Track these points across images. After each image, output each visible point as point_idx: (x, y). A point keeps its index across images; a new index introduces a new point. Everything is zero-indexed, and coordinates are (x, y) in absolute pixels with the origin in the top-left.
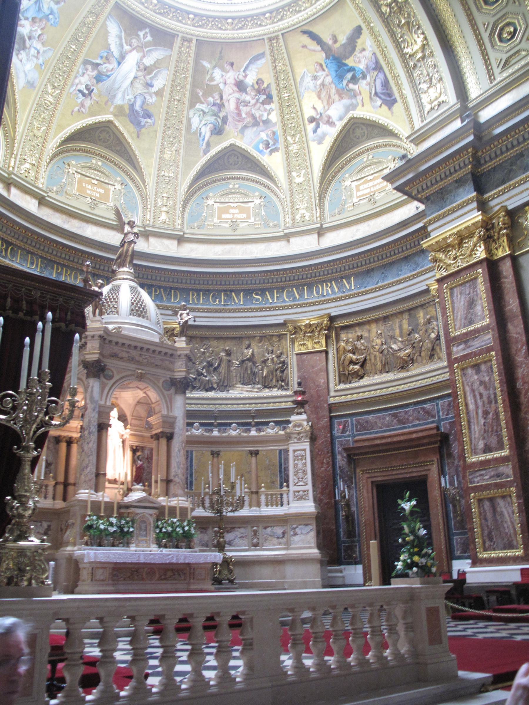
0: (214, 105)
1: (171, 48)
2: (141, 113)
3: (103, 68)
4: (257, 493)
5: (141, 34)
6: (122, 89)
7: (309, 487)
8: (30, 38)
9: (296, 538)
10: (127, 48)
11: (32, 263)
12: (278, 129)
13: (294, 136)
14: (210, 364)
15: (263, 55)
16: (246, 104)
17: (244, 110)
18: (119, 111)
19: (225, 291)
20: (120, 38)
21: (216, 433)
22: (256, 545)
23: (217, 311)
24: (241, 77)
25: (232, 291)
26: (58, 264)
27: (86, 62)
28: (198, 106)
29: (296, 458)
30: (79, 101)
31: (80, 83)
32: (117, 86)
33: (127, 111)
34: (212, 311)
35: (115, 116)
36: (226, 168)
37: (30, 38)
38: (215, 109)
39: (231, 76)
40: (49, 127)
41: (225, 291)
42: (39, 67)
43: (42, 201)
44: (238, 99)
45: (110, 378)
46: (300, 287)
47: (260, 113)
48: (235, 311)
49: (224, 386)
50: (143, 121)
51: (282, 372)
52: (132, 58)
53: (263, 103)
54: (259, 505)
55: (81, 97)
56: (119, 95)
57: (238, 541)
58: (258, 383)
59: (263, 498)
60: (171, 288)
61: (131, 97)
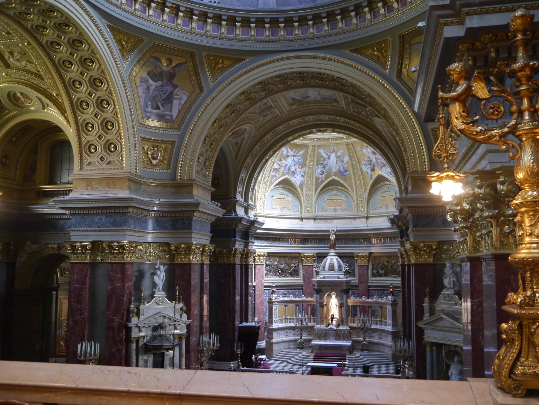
0: (368, 161)
2: (344, 171)
3: (324, 163)
4: (382, 321)
6: (334, 166)
7: (391, 322)
8: (295, 170)
9: (388, 338)
10: (329, 154)
11: (315, 242)
16: (379, 159)
17: (379, 161)
19: (383, 238)
20: (325, 152)
22: (380, 338)
25: (386, 238)
26: (324, 239)
27: (317, 165)
28: (363, 163)
30: (320, 177)
31: (318, 171)
32: (331, 166)
33: (338, 172)
37: (295, 170)
38: (369, 162)
40: (312, 192)
41: (383, 238)
42: (302, 176)
43: (315, 219)
44: (375, 157)
45: (322, 292)
49: (386, 275)
50: (345, 174)
52: (333, 156)
55: (320, 176)
56: (334, 169)
57: (376, 336)
58: (396, 274)
60: (366, 238)
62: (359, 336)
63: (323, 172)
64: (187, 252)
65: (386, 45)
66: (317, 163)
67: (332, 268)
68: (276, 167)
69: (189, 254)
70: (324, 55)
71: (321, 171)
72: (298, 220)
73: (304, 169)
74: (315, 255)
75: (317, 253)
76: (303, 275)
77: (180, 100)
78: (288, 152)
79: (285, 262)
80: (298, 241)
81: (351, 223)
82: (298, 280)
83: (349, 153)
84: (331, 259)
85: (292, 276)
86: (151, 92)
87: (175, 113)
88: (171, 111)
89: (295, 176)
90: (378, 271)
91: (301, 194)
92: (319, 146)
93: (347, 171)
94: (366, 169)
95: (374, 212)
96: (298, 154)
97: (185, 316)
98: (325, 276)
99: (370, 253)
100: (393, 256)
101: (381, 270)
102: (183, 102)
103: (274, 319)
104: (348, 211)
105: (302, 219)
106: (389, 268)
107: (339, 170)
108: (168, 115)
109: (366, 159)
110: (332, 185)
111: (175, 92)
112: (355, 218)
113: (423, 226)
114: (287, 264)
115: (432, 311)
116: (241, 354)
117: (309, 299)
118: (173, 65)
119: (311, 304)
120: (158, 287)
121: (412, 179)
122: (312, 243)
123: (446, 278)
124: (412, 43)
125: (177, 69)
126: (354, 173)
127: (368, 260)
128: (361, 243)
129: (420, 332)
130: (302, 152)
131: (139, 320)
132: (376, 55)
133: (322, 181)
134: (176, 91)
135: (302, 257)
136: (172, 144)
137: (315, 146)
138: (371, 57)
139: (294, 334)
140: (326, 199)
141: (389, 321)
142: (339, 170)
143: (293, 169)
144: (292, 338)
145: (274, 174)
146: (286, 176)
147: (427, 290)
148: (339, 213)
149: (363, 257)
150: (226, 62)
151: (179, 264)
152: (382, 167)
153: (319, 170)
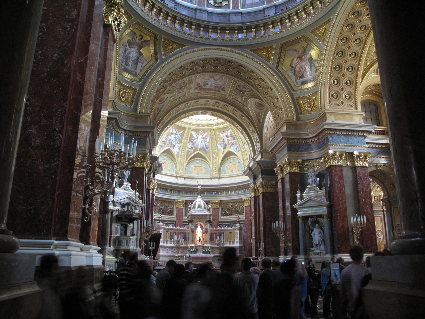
1: (208, 132)
3: (194, 141)
4: (231, 241)
5: (200, 132)
7: (238, 241)
10: (198, 135)
12: (238, 145)
13: (242, 147)
14: (228, 209)
15: (229, 129)
16: (230, 140)
17: (230, 142)
18: (200, 149)
20: (196, 134)
21: (223, 228)
23: (228, 196)
24: (227, 134)
27: (189, 142)
29: (237, 234)
34: (227, 196)
35: (199, 150)
36: (230, 156)
38: (223, 142)
39: (224, 134)
42: (179, 149)
43: (185, 178)
46: (245, 189)
47: (234, 142)
48: (232, 196)
49: (231, 214)
50: (206, 150)
51: (243, 210)
52: (200, 137)
53: (233, 139)
54: (231, 244)
55: (190, 150)
56: (199, 146)
59: (232, 243)
61: (202, 145)
62: (215, 253)
63: (192, 148)
64: (142, 160)
65: (271, 49)
66: (189, 140)
67: (199, 207)
68: (164, 140)
69: (143, 162)
70: (235, 50)
71: (191, 147)
72: (174, 178)
73: (181, 144)
74: (184, 202)
75: (186, 201)
76: (176, 214)
77: (143, 63)
78: (173, 131)
79: (165, 205)
80: (173, 192)
81: (209, 181)
82: (173, 218)
83: (211, 136)
84: (200, 201)
85: (169, 215)
86: (127, 54)
87: (138, 71)
88: (136, 69)
89: (175, 148)
90: (226, 212)
91: (177, 161)
92: (193, 130)
93: (208, 148)
94: (221, 147)
95: (224, 175)
96: (179, 134)
97: (141, 201)
98: (196, 211)
99: (221, 201)
100: (236, 202)
101: (228, 211)
102: (144, 65)
103: (161, 240)
104: (206, 174)
105: (177, 177)
106: (233, 210)
107: (203, 147)
108: (134, 72)
109: (221, 141)
110: (196, 157)
111: (140, 58)
112: (211, 178)
113: (293, 151)
114: (166, 206)
115: (302, 198)
116: (153, 250)
117: (182, 228)
118: (143, 40)
119: (183, 232)
120: (126, 178)
121: (287, 125)
122: (183, 193)
123: (309, 178)
124: (287, 49)
125: (144, 43)
126: (212, 150)
127: (219, 205)
128: (215, 194)
129: (294, 211)
130: (181, 132)
131: (114, 198)
132: (265, 55)
133: (191, 154)
134: (141, 57)
135: (175, 202)
136: (135, 90)
137: (190, 129)
138: (262, 55)
139: (172, 252)
140: (192, 166)
141: (237, 240)
142: (203, 147)
143: (174, 143)
144: (171, 254)
145: (162, 145)
146: (169, 147)
147: (299, 186)
148: (200, 175)
149: (216, 203)
150: (174, 45)
151: (136, 168)
152: (231, 146)
153: (190, 145)
